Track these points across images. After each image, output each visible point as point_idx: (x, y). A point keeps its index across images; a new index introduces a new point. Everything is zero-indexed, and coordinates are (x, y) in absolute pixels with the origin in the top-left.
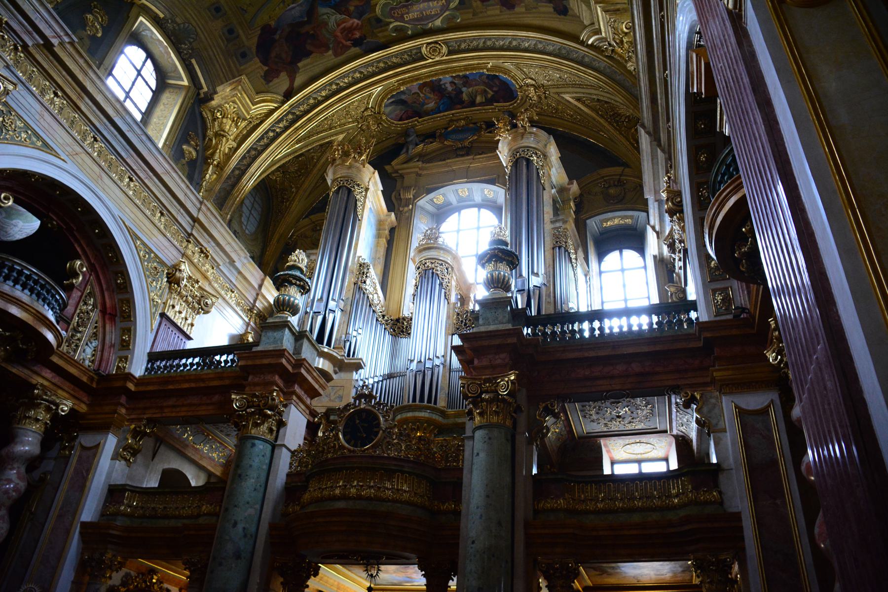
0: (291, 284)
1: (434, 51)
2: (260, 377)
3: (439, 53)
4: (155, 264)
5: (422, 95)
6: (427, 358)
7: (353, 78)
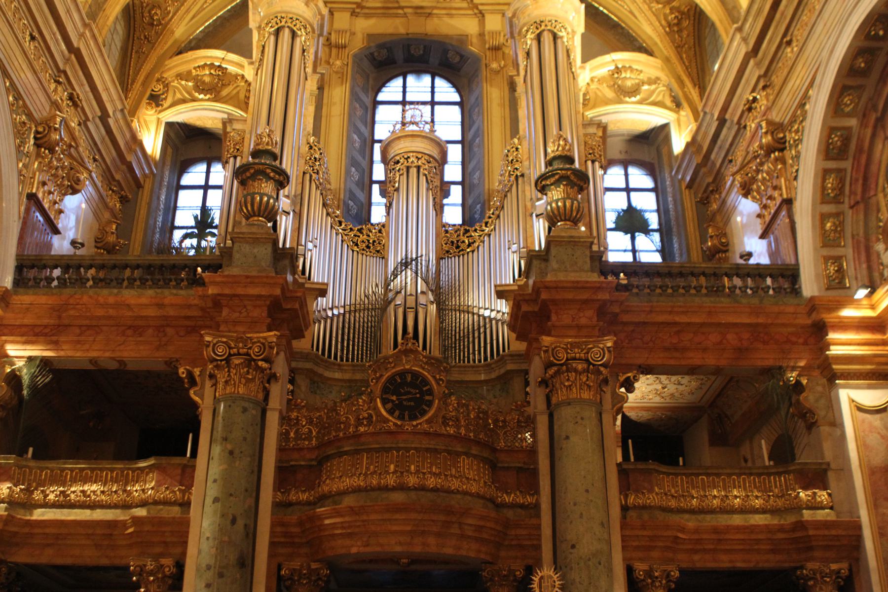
0: (269, 178)
2: (240, 312)
4: (24, 117)
6: (419, 291)
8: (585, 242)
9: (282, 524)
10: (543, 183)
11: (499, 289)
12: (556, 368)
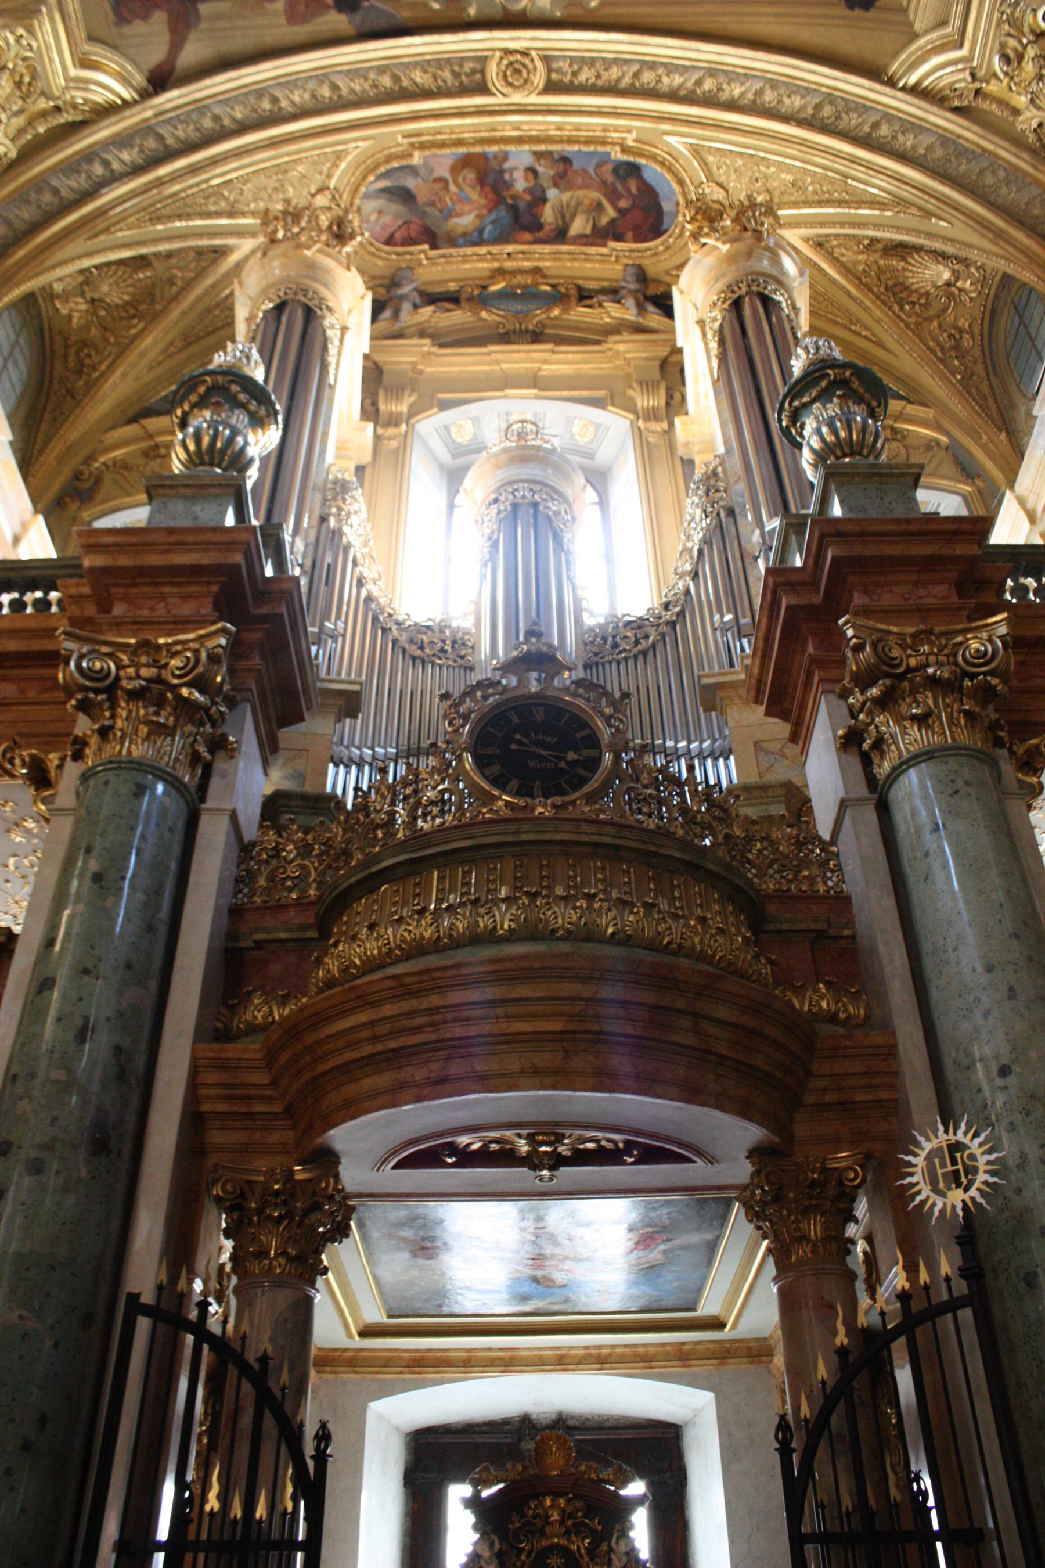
1: (518, 72)
2: (152, 609)
3: (526, 81)
5: (453, 188)
7: (313, 96)
8: (904, 474)
9: (221, 1065)
10: (796, 403)
11: (705, 681)
12: (888, 682)
